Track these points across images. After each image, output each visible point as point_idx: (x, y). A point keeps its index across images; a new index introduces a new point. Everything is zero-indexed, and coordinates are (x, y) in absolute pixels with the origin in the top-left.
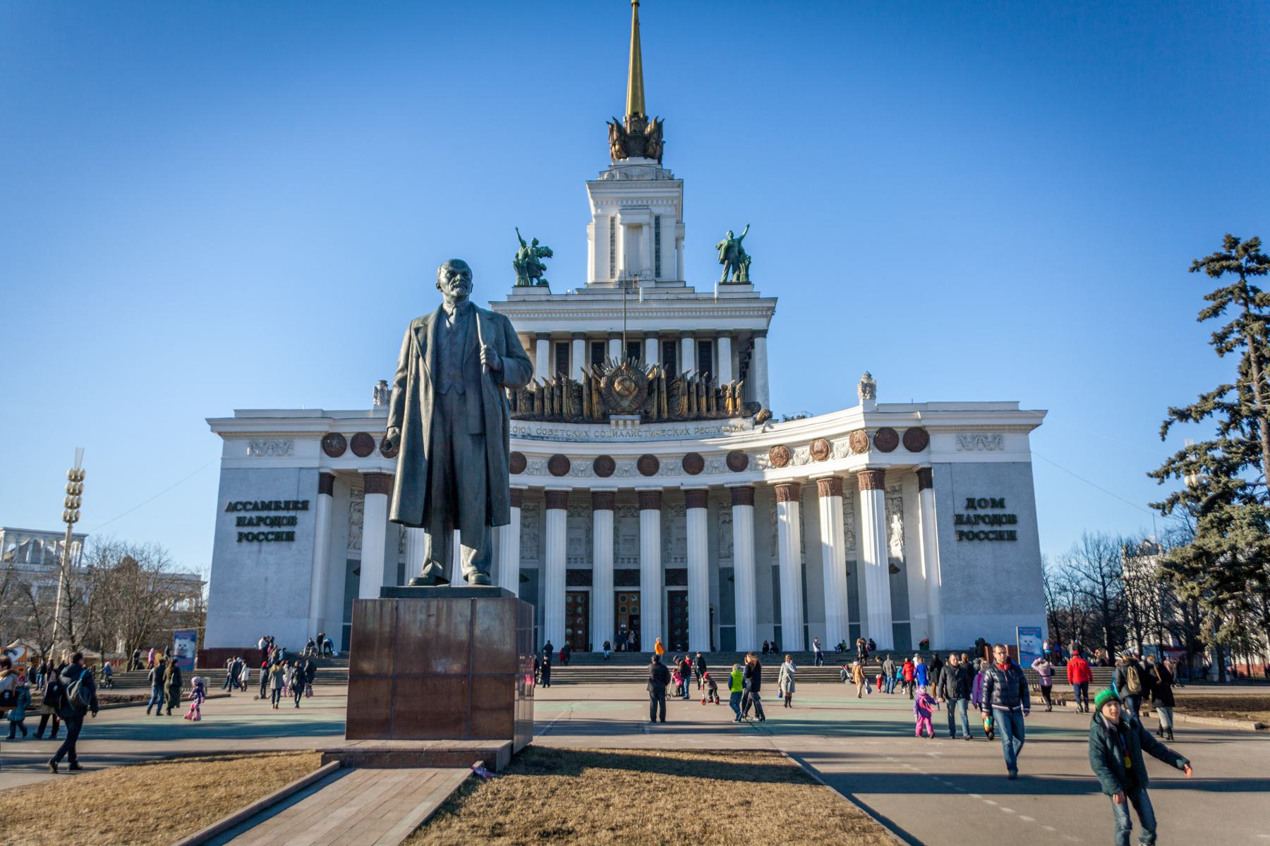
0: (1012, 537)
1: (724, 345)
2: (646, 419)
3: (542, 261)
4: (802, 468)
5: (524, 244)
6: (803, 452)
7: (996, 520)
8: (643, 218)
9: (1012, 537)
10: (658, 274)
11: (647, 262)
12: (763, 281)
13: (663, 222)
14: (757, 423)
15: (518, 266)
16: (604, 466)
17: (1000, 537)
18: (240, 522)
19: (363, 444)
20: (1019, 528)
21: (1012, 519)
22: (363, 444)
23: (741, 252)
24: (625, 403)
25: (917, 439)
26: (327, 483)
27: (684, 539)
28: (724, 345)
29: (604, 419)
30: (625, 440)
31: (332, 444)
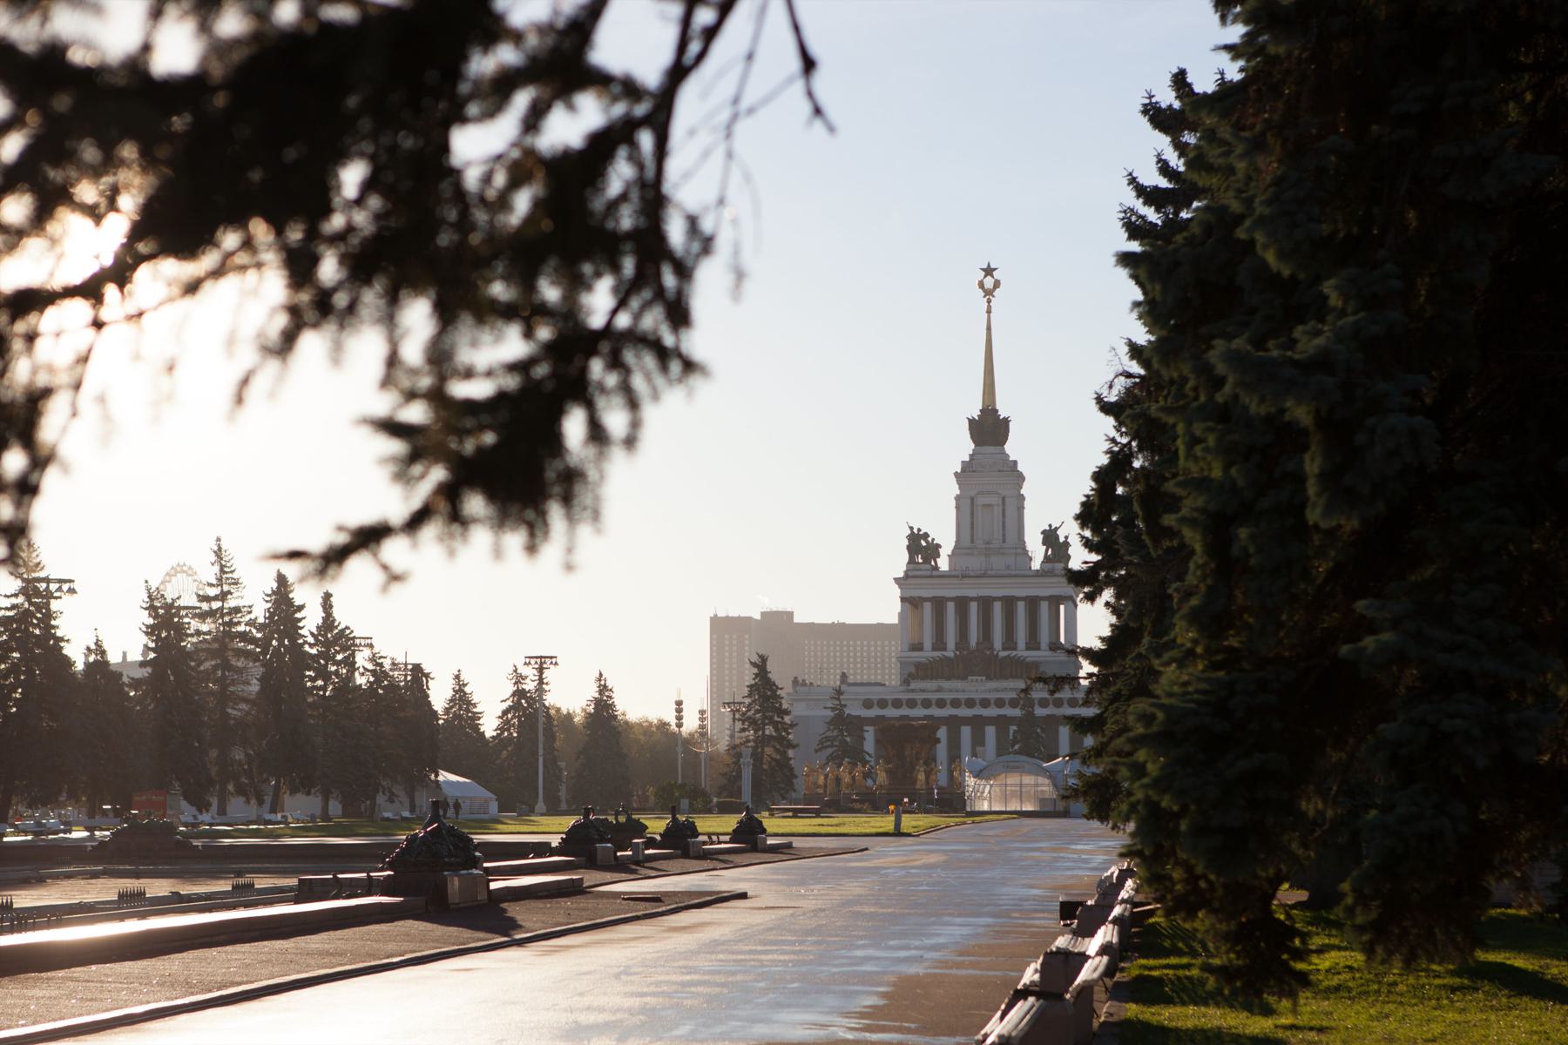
2: (989, 678)
8: (995, 500)
13: (1008, 501)
29: (964, 678)
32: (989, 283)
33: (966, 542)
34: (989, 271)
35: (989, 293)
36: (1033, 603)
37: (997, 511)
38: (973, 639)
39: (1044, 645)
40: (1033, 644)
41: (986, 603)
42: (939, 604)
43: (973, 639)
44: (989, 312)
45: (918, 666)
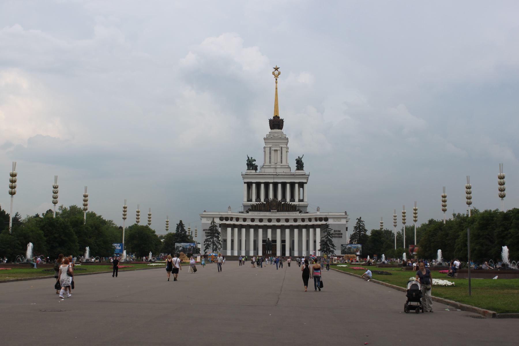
0: (341, 237)
1: (297, 185)
2: (278, 211)
3: (254, 163)
4: (307, 223)
5: (248, 157)
6: (307, 220)
7: (339, 234)
9: (341, 237)
10: (281, 163)
11: (279, 160)
12: (306, 169)
13: (283, 149)
14: (300, 213)
15: (247, 164)
16: (270, 220)
17: (339, 237)
18: (206, 233)
19: (227, 219)
20: (343, 236)
21: (342, 234)
22: (227, 219)
23: (301, 161)
24: (274, 208)
25: (326, 219)
26: (221, 225)
27: (285, 234)
28: (297, 185)
29: (270, 211)
30: (274, 215)
31: (221, 219)
32: (276, 72)
33: (267, 163)
34: (276, 69)
35: (276, 77)
36: (292, 185)
37: (279, 152)
38: (271, 196)
39: (297, 199)
40: (292, 198)
41: (275, 185)
42: (258, 185)
43: (271, 196)
44: (276, 83)
45: (252, 206)
